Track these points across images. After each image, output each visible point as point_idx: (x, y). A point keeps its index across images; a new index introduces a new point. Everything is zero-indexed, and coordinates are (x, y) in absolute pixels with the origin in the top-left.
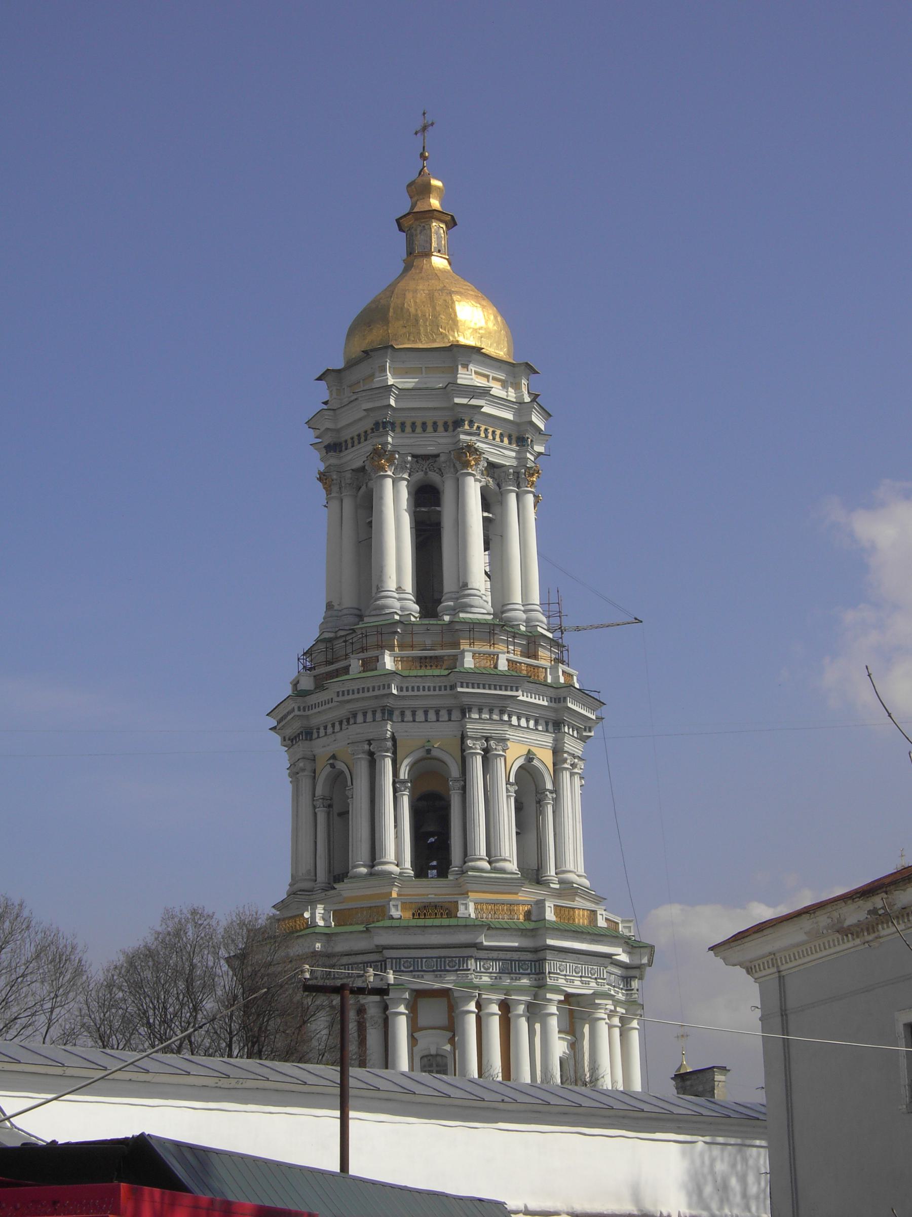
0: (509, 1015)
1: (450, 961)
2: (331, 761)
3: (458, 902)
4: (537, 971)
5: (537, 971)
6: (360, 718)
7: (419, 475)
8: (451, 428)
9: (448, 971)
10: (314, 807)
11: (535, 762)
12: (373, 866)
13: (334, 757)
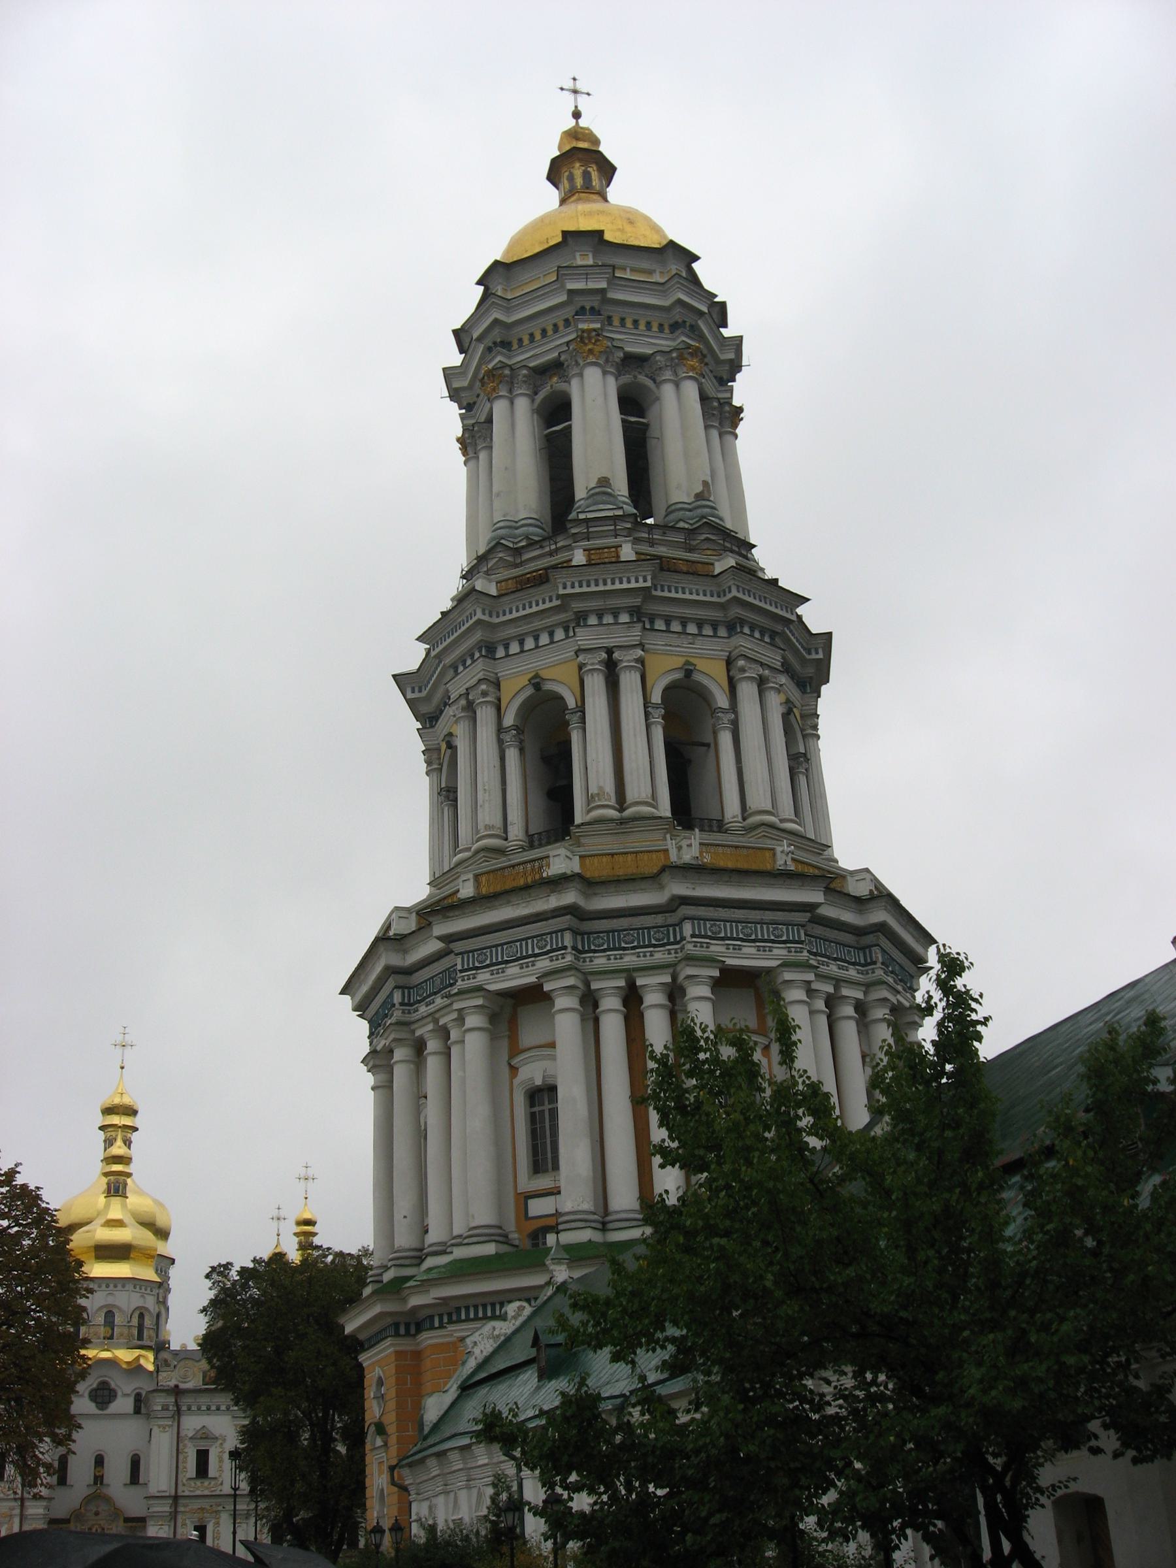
0: (833, 1017)
1: (775, 929)
2: (538, 680)
3: (773, 849)
4: (862, 961)
5: (862, 961)
6: (593, 620)
7: (626, 379)
8: (667, 331)
9: (773, 942)
10: (500, 742)
11: (792, 717)
12: (622, 809)
13: (537, 676)
